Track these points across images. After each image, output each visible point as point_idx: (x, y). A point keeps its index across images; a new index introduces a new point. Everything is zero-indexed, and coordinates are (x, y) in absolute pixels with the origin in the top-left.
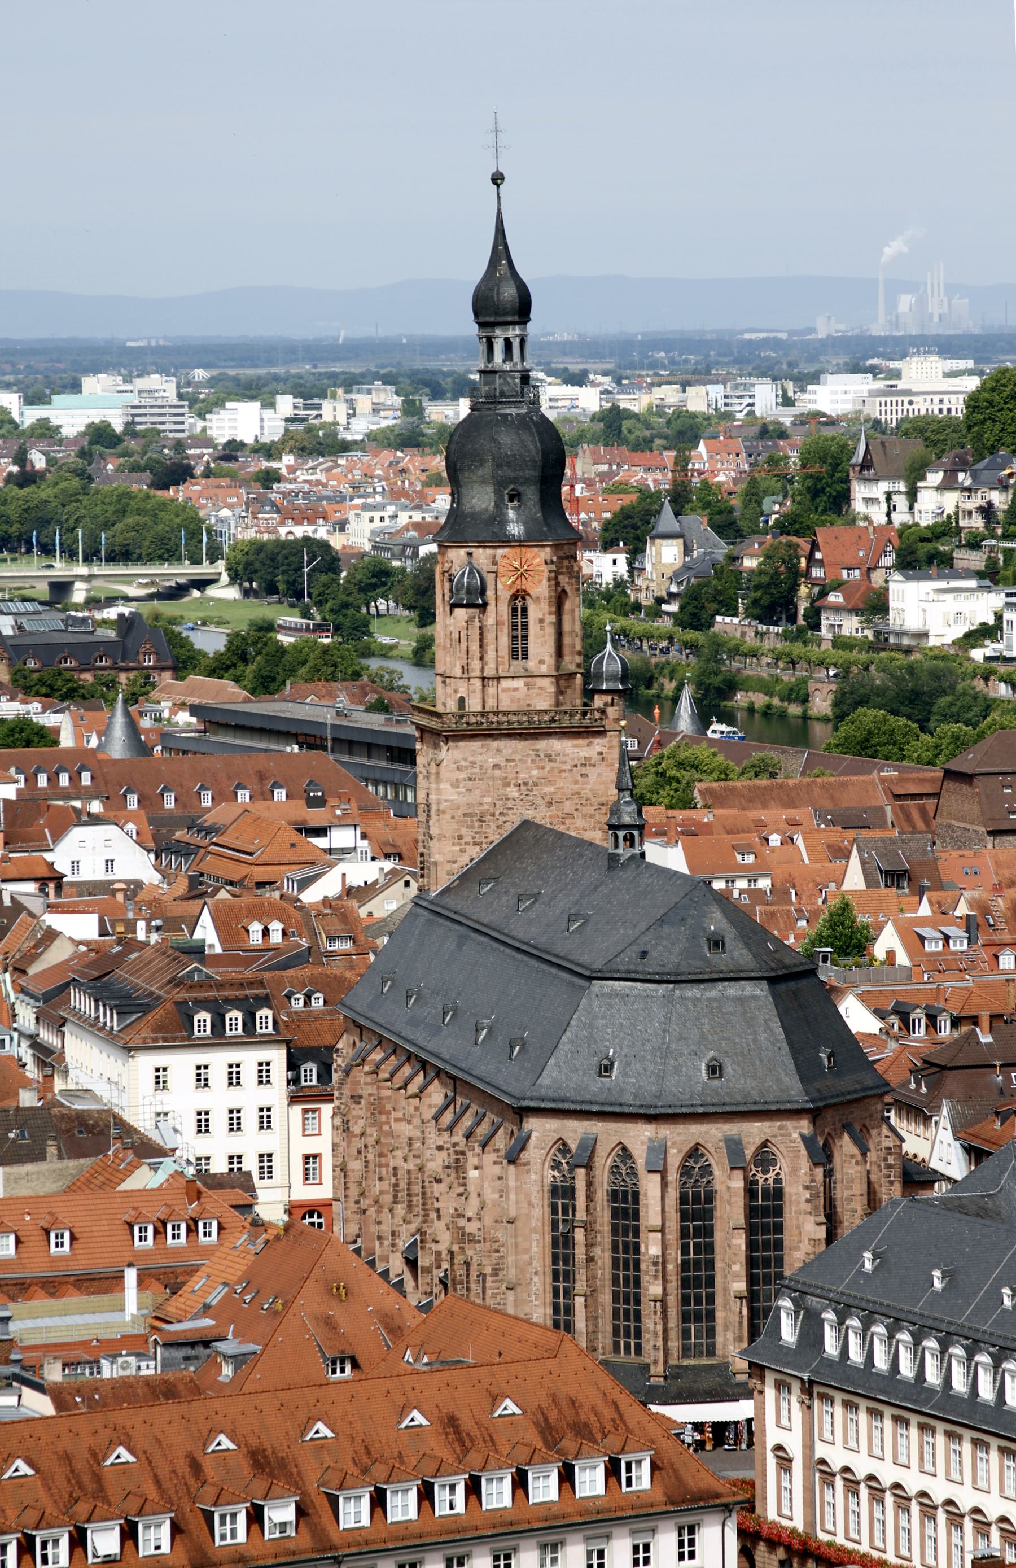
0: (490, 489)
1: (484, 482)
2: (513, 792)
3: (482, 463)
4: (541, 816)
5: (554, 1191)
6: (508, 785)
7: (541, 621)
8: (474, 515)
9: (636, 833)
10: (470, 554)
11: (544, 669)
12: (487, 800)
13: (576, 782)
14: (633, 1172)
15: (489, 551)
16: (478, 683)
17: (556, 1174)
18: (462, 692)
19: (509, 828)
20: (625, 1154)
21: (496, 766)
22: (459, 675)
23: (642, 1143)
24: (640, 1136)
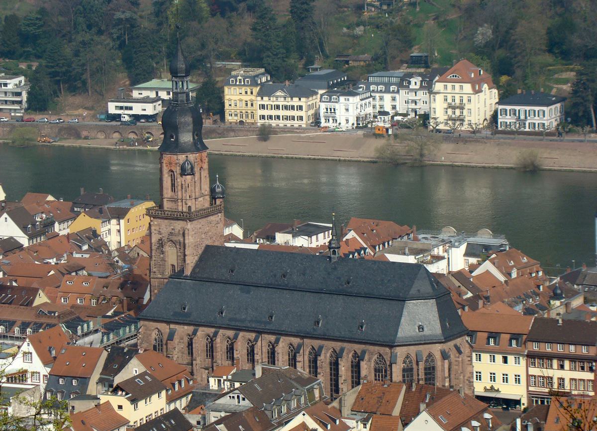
0: (191, 134)
1: (189, 131)
2: (203, 236)
3: (188, 125)
4: (209, 242)
5: (404, 370)
6: (202, 234)
7: (206, 177)
8: (185, 143)
9: (336, 250)
10: (187, 157)
11: (206, 193)
12: (199, 240)
13: (216, 230)
14: (433, 361)
15: (194, 155)
16: (194, 200)
17: (404, 365)
18: (189, 204)
19: (203, 248)
20: (430, 355)
21: (200, 228)
22: (188, 198)
23: (438, 351)
24: (436, 349)
